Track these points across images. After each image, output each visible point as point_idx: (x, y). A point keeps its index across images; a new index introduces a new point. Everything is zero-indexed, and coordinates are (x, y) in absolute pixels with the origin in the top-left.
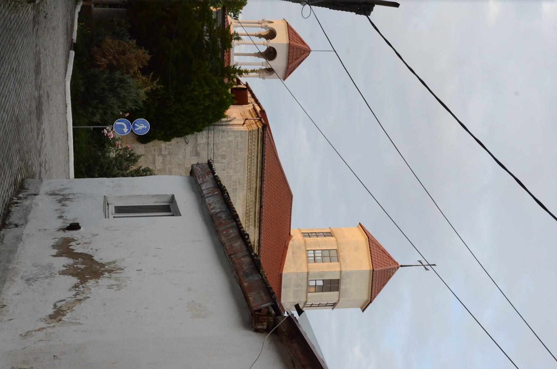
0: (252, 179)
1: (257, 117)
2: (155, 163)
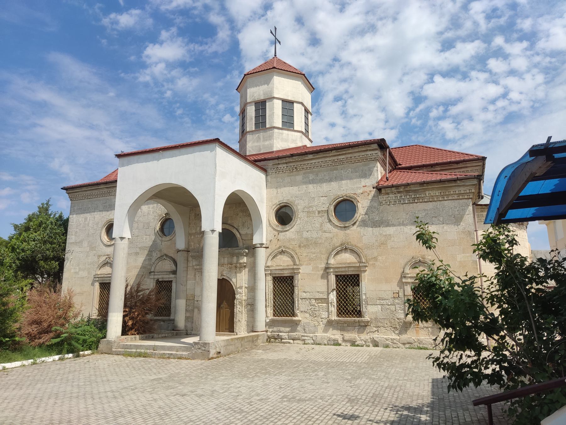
2: (83, 277)
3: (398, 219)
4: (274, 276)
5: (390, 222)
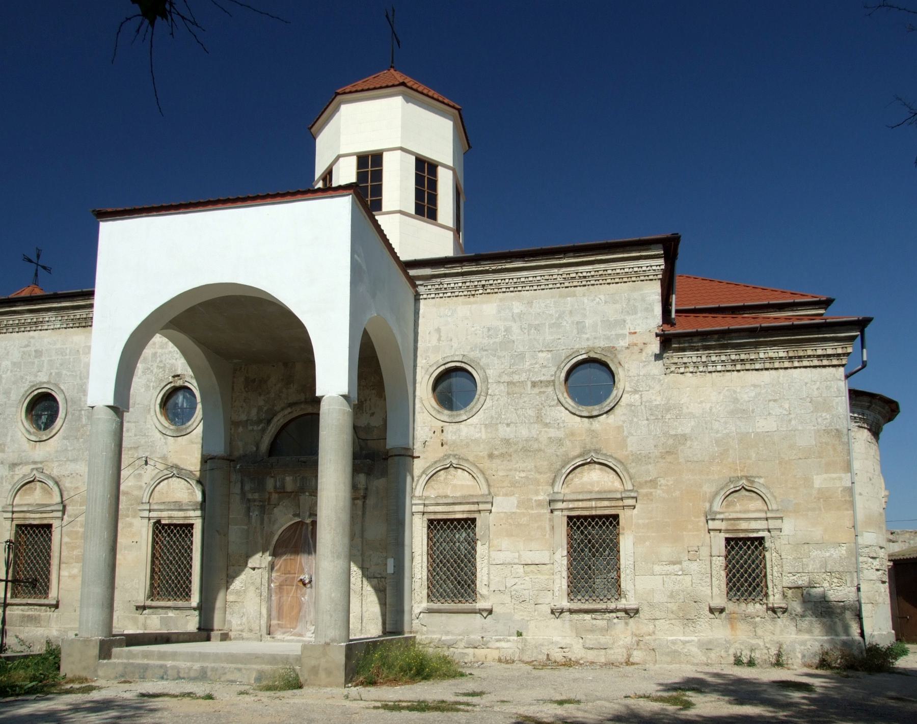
3: (701, 402)
4: (432, 517)
5: (685, 408)
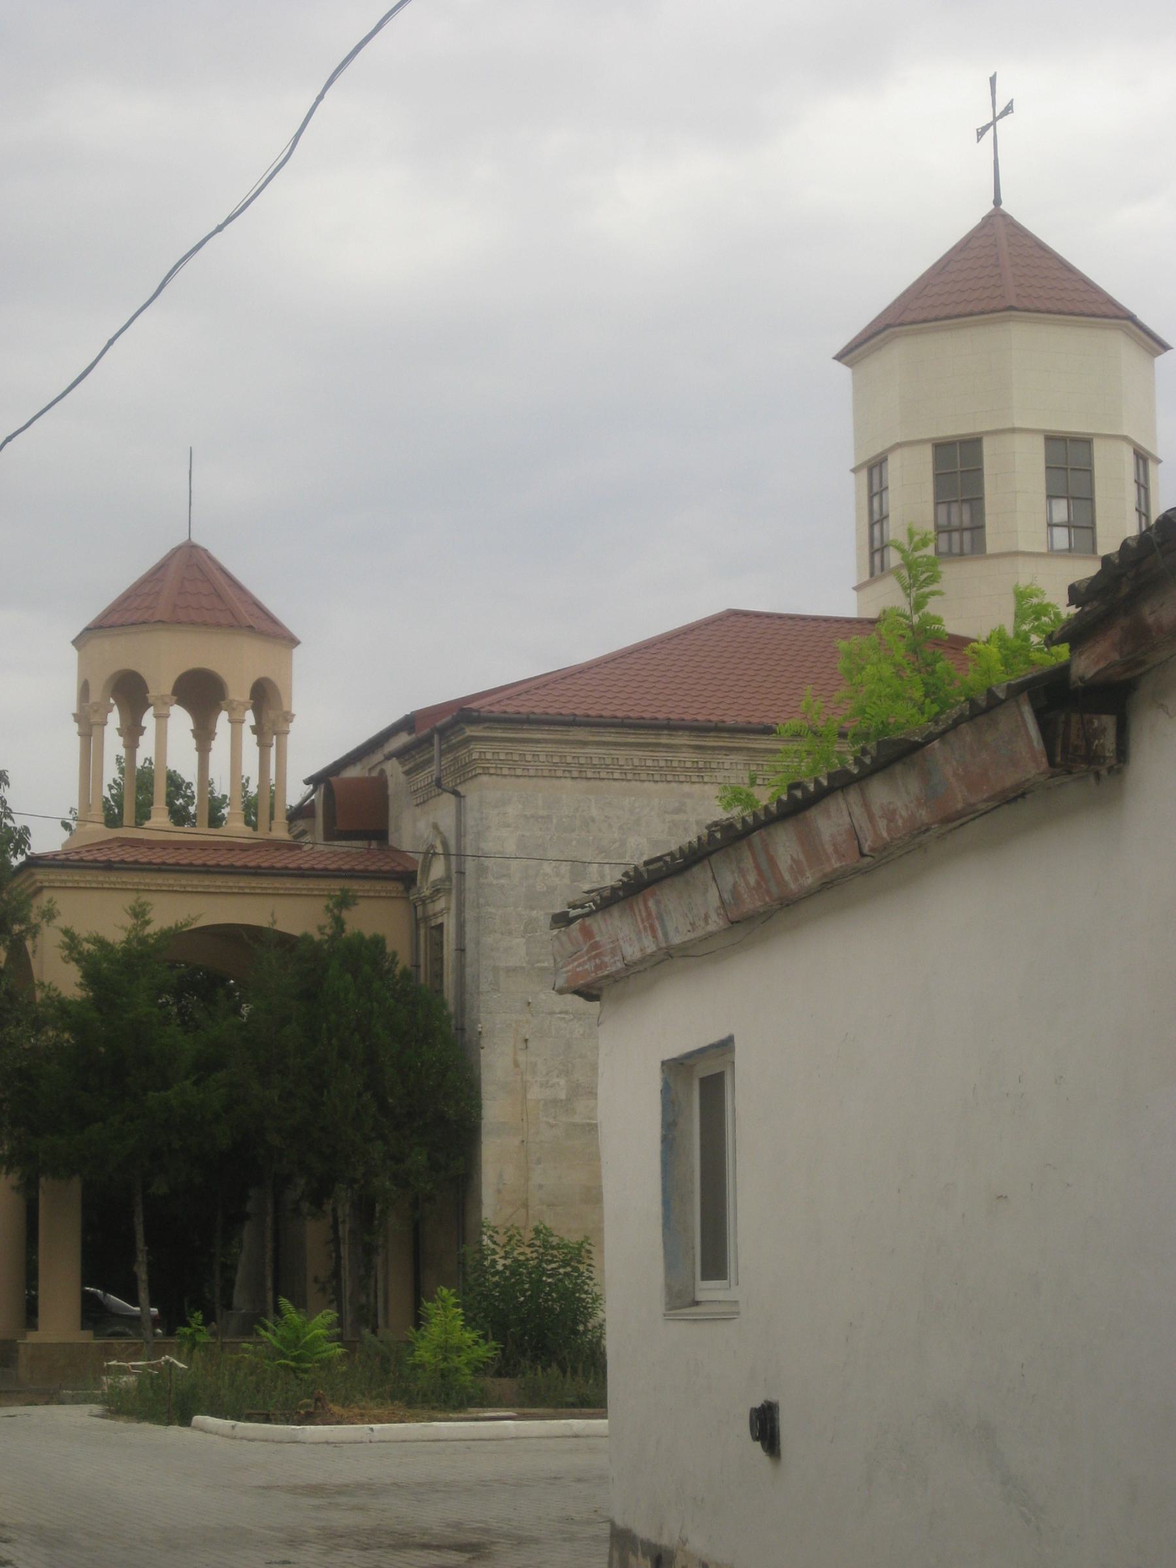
0: (662, 764)
1: (432, 745)
